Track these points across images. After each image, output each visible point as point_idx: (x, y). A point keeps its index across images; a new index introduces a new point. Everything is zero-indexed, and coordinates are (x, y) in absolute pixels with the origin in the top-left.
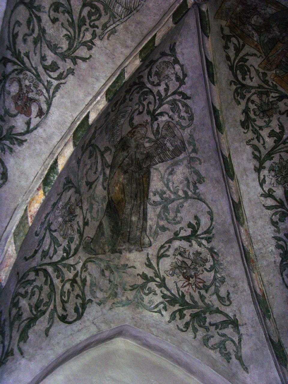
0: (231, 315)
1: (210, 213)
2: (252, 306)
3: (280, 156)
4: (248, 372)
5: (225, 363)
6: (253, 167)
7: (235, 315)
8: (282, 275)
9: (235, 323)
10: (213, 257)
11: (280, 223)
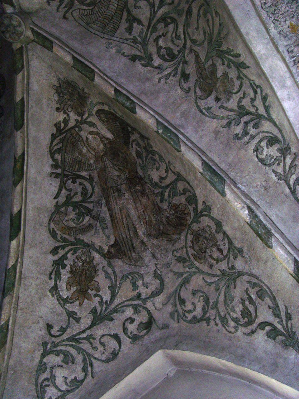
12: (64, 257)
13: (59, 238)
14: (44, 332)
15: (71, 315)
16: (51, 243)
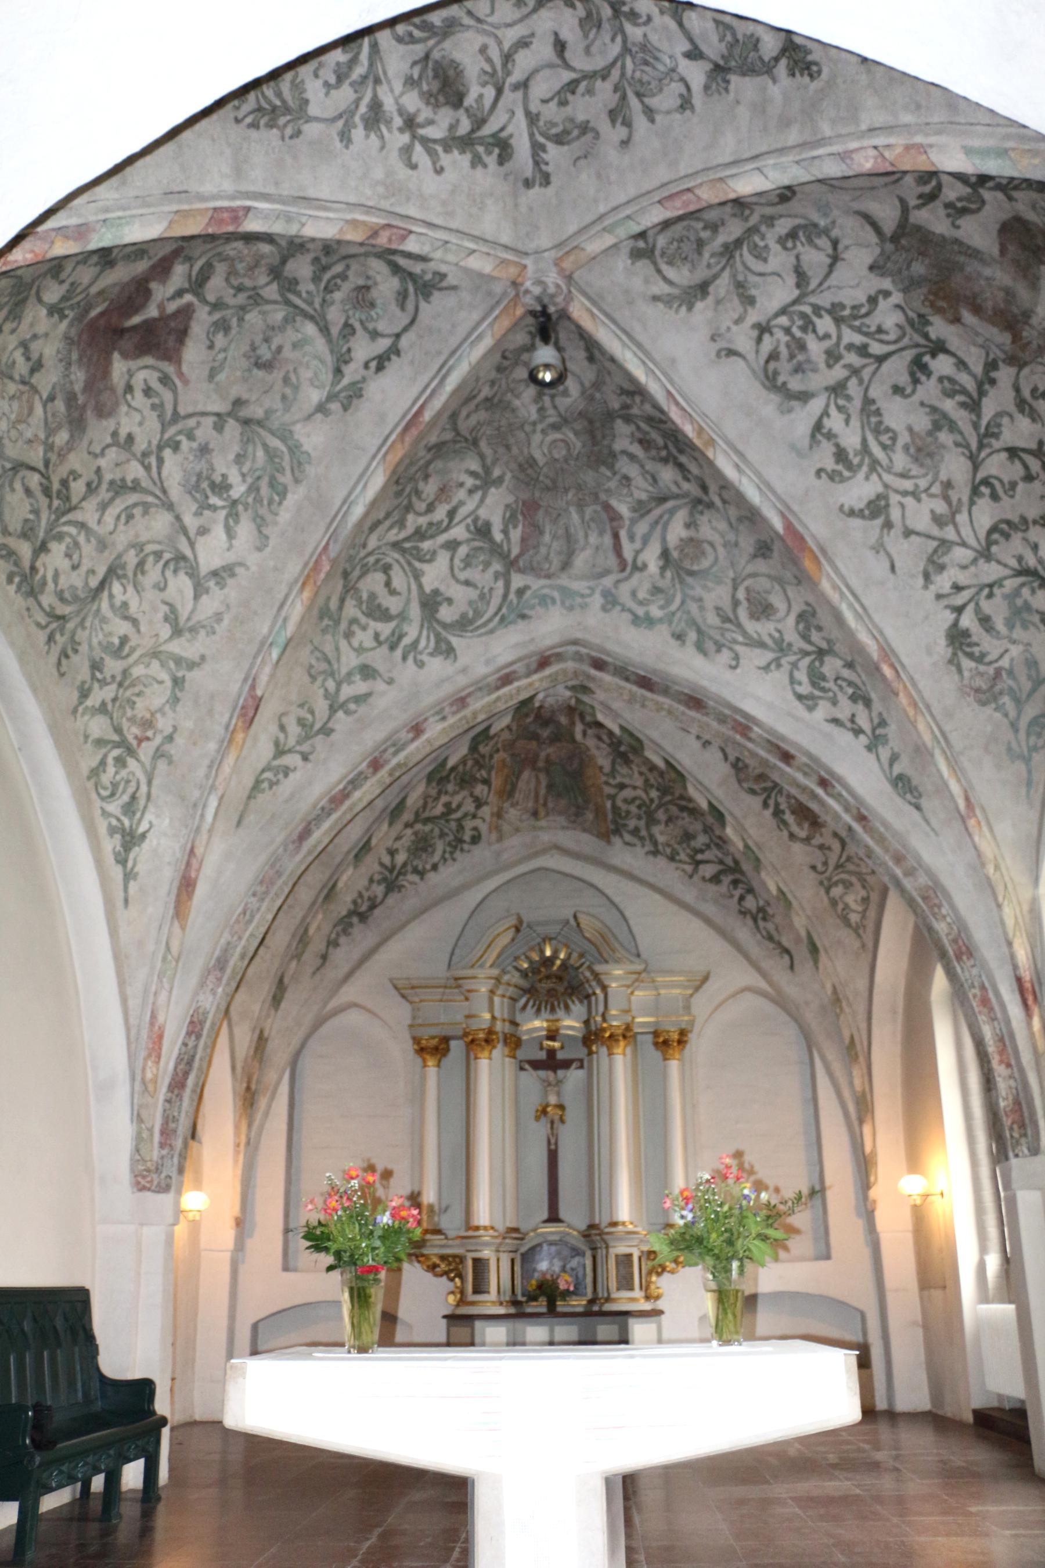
2: (288, 938)
12: (777, 804)
14: (813, 875)
15: (821, 847)
16: (756, 802)
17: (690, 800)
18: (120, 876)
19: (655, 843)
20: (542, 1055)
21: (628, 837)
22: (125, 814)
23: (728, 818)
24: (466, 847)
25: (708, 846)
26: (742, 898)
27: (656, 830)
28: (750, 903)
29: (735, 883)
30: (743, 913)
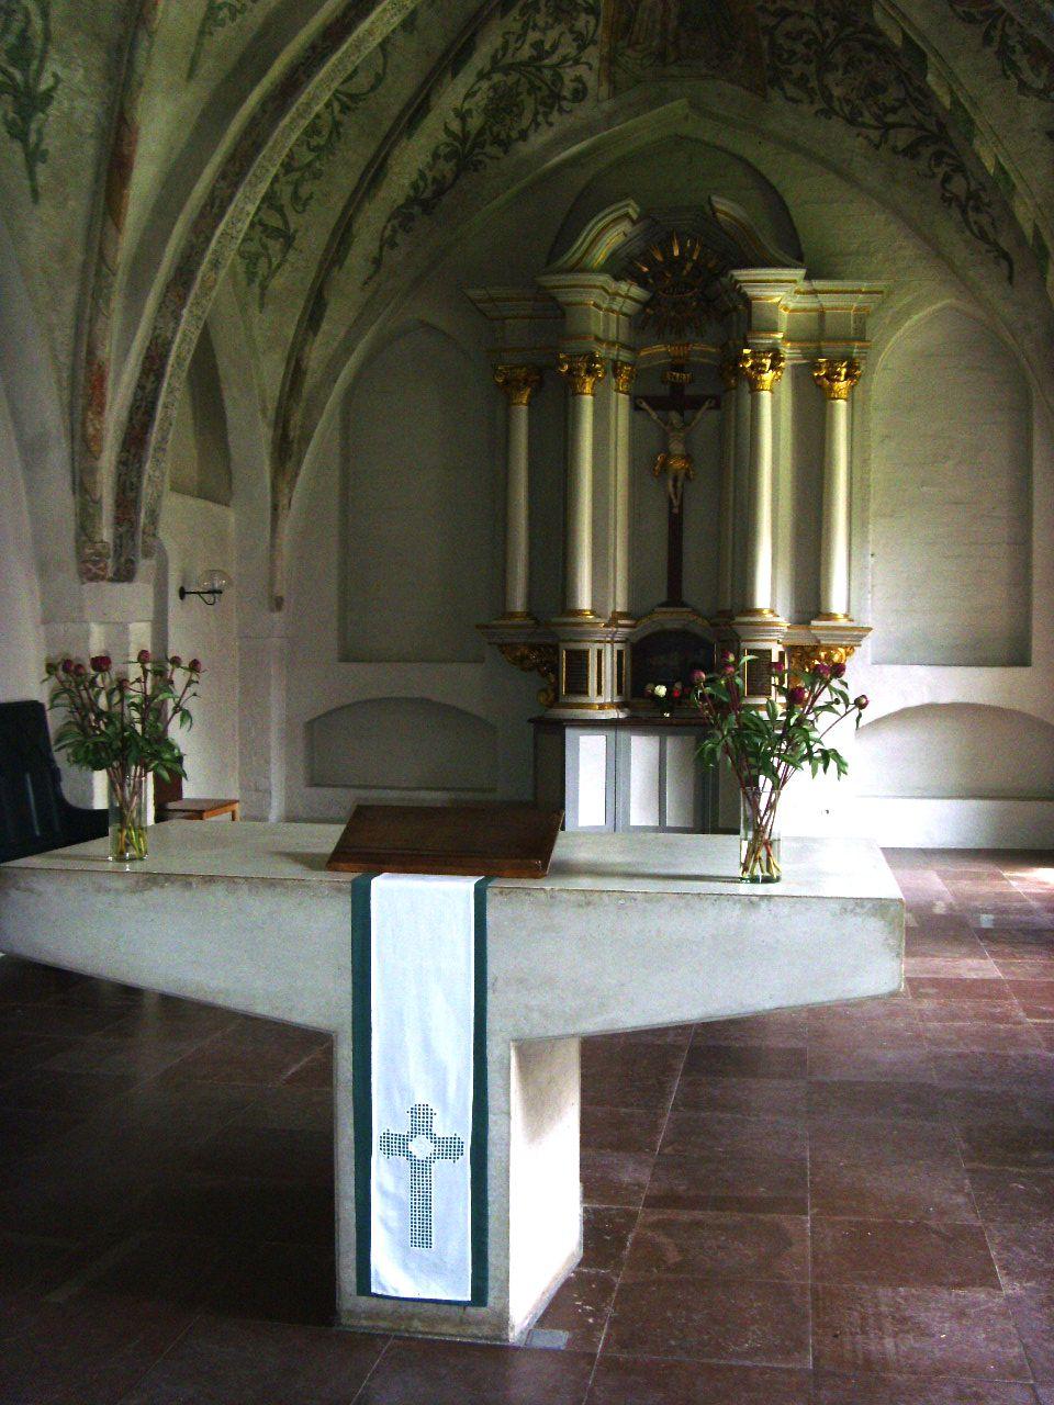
0: (293, 226)
1: (379, 79)
3: (519, 80)
4: (261, 312)
5: (244, 283)
6: (480, 67)
7: (296, 231)
8: (389, 221)
9: (288, 240)
10: (330, 136)
11: (441, 160)
13: (979, 17)
17: (881, 34)
18: (20, 158)
19: (829, 98)
20: (664, 390)
21: (791, 90)
22: (14, 63)
23: (932, 59)
24: (566, 105)
25: (903, 103)
26: (947, 179)
27: (830, 79)
28: (958, 185)
29: (938, 157)
30: (948, 200)
